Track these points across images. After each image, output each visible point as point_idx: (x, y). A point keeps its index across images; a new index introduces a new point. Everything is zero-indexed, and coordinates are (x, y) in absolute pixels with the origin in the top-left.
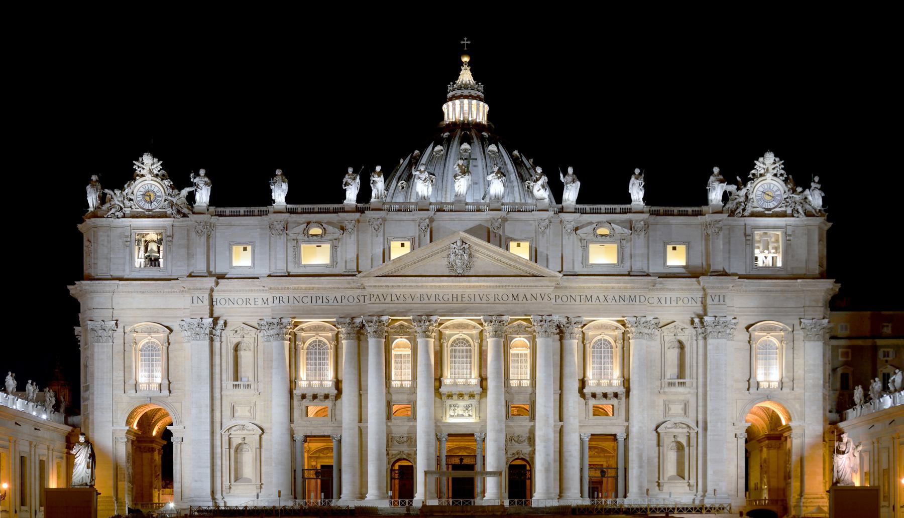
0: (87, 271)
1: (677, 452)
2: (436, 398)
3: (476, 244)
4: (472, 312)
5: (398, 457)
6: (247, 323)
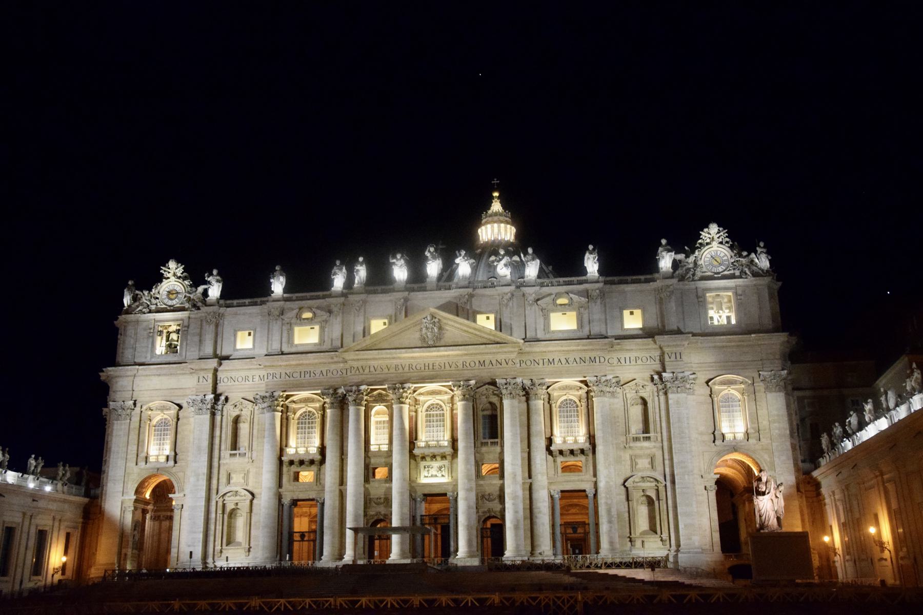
0: (119, 359)
2: (411, 460)
3: (445, 318)
4: (443, 378)
5: (376, 518)
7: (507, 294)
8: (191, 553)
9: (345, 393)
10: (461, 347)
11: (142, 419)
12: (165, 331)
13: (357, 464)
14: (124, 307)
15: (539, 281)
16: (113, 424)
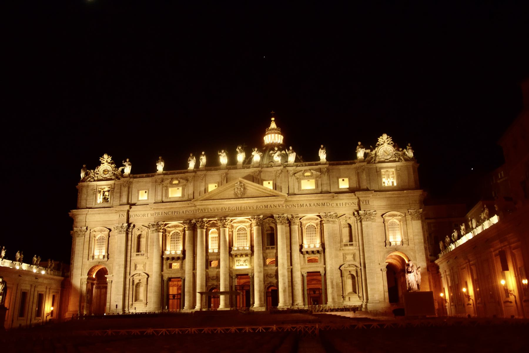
0: (78, 206)
1: (352, 279)
2: (230, 257)
3: (247, 183)
4: (246, 214)
6: (144, 225)
7: (279, 170)
8: (117, 305)
9: (195, 222)
10: (255, 198)
11: (91, 236)
12: (102, 191)
13: (202, 259)
14: (81, 178)
15: (295, 164)
16: (76, 239)
